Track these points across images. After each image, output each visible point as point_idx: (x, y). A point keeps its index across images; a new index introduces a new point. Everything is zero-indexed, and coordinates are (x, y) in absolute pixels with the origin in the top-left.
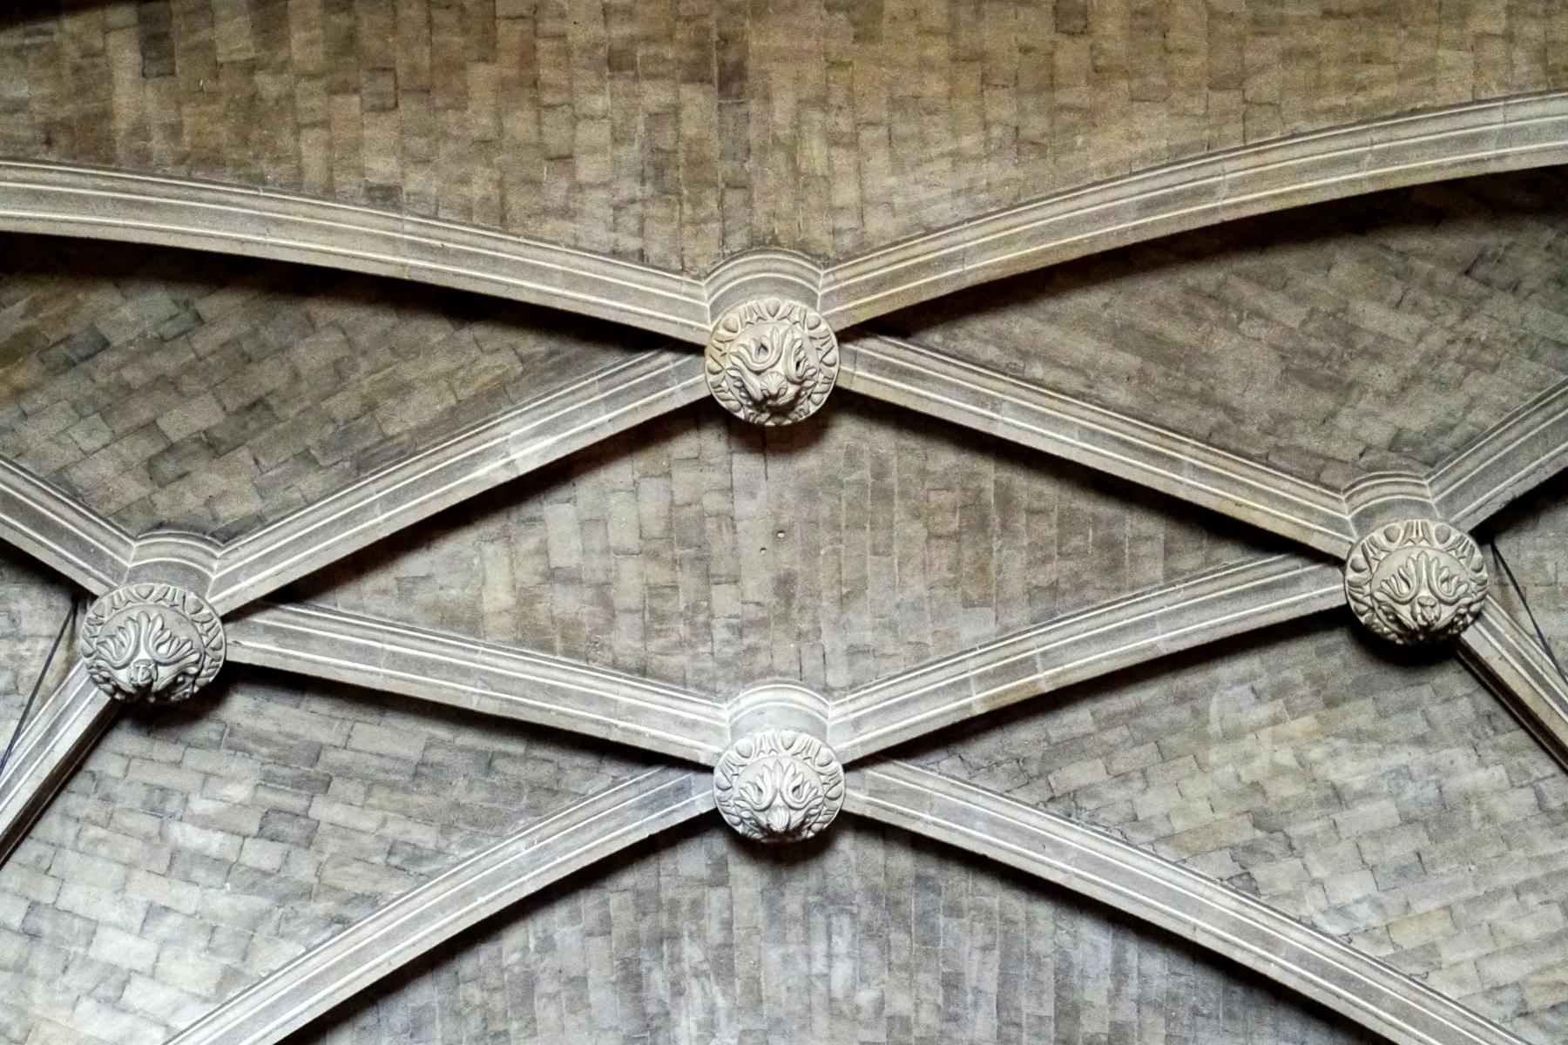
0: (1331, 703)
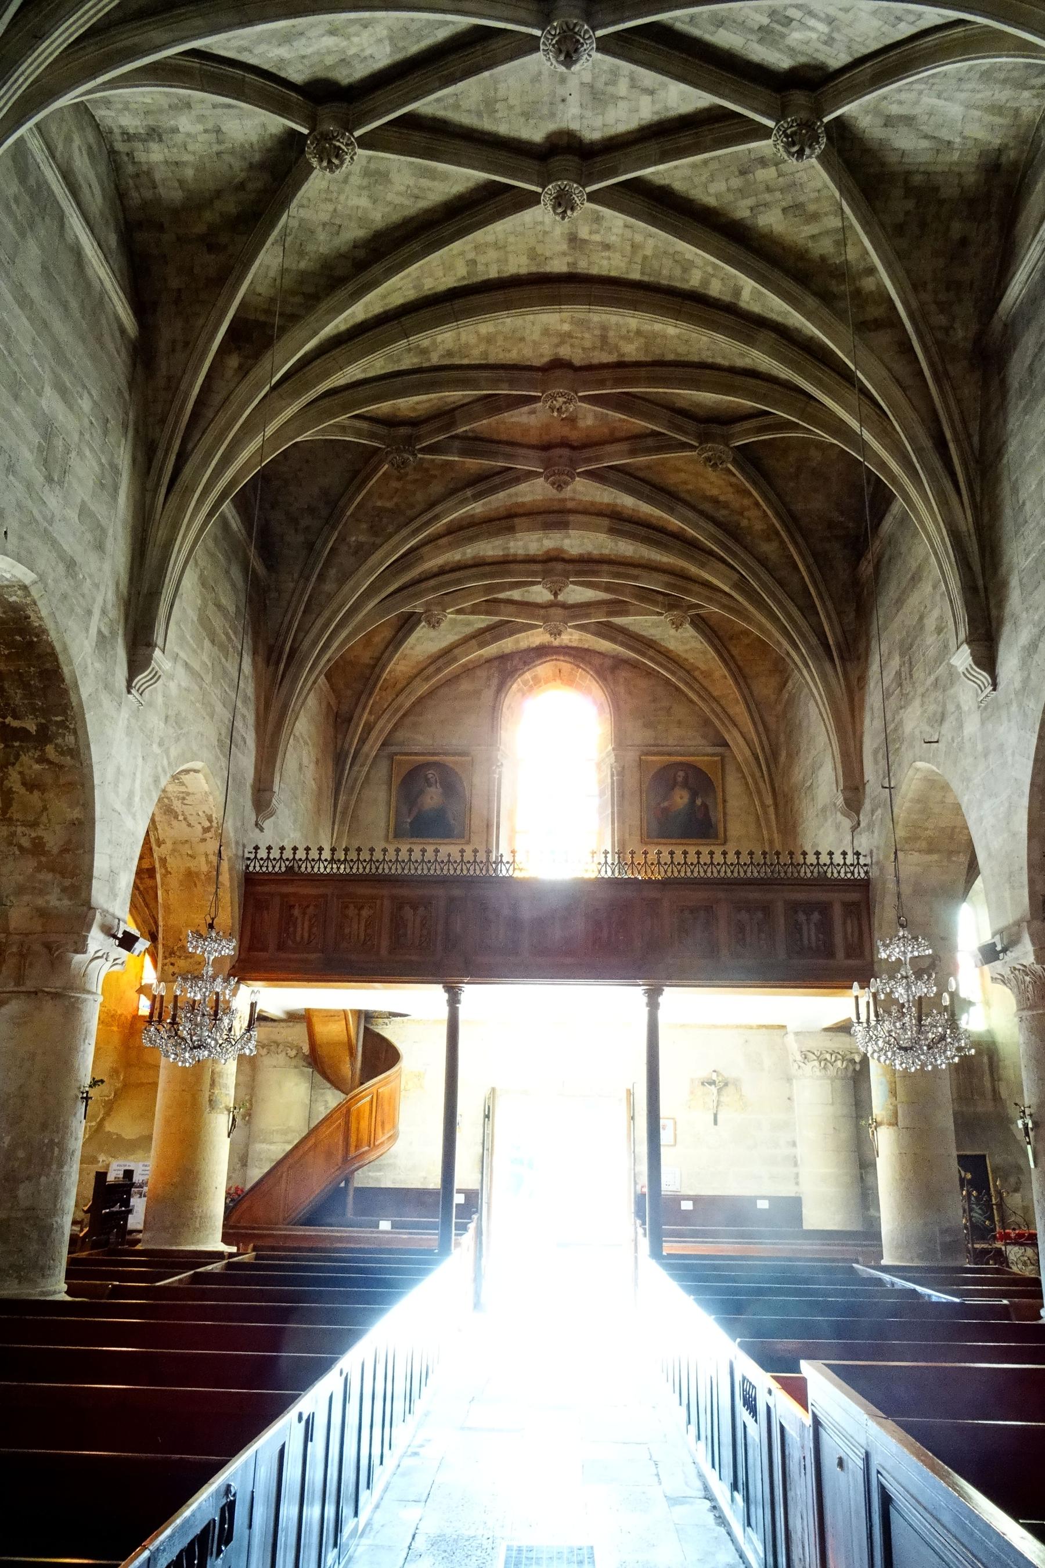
0: (343, 60)
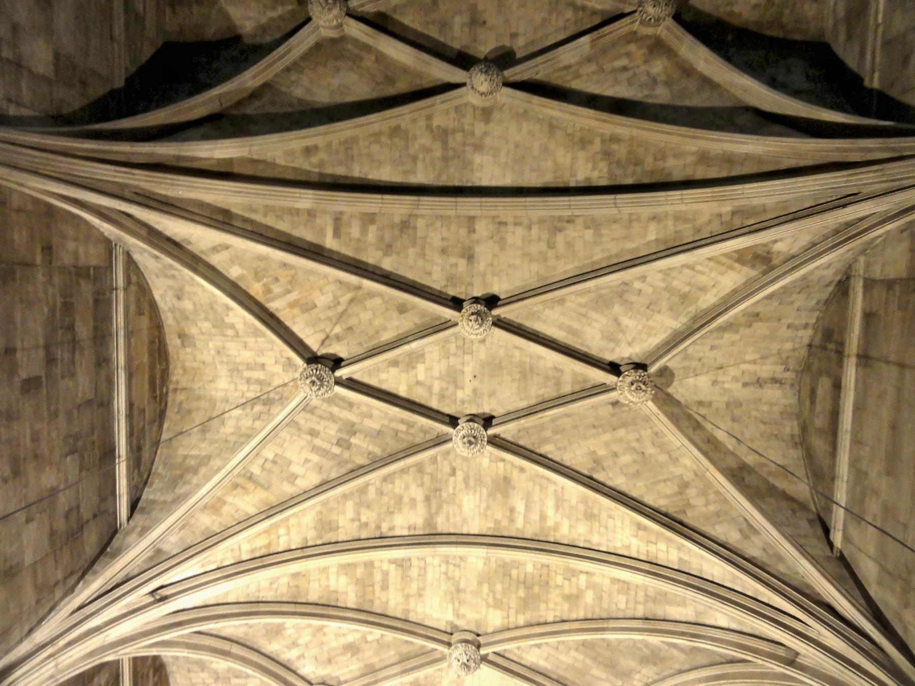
0: (614, 429)
